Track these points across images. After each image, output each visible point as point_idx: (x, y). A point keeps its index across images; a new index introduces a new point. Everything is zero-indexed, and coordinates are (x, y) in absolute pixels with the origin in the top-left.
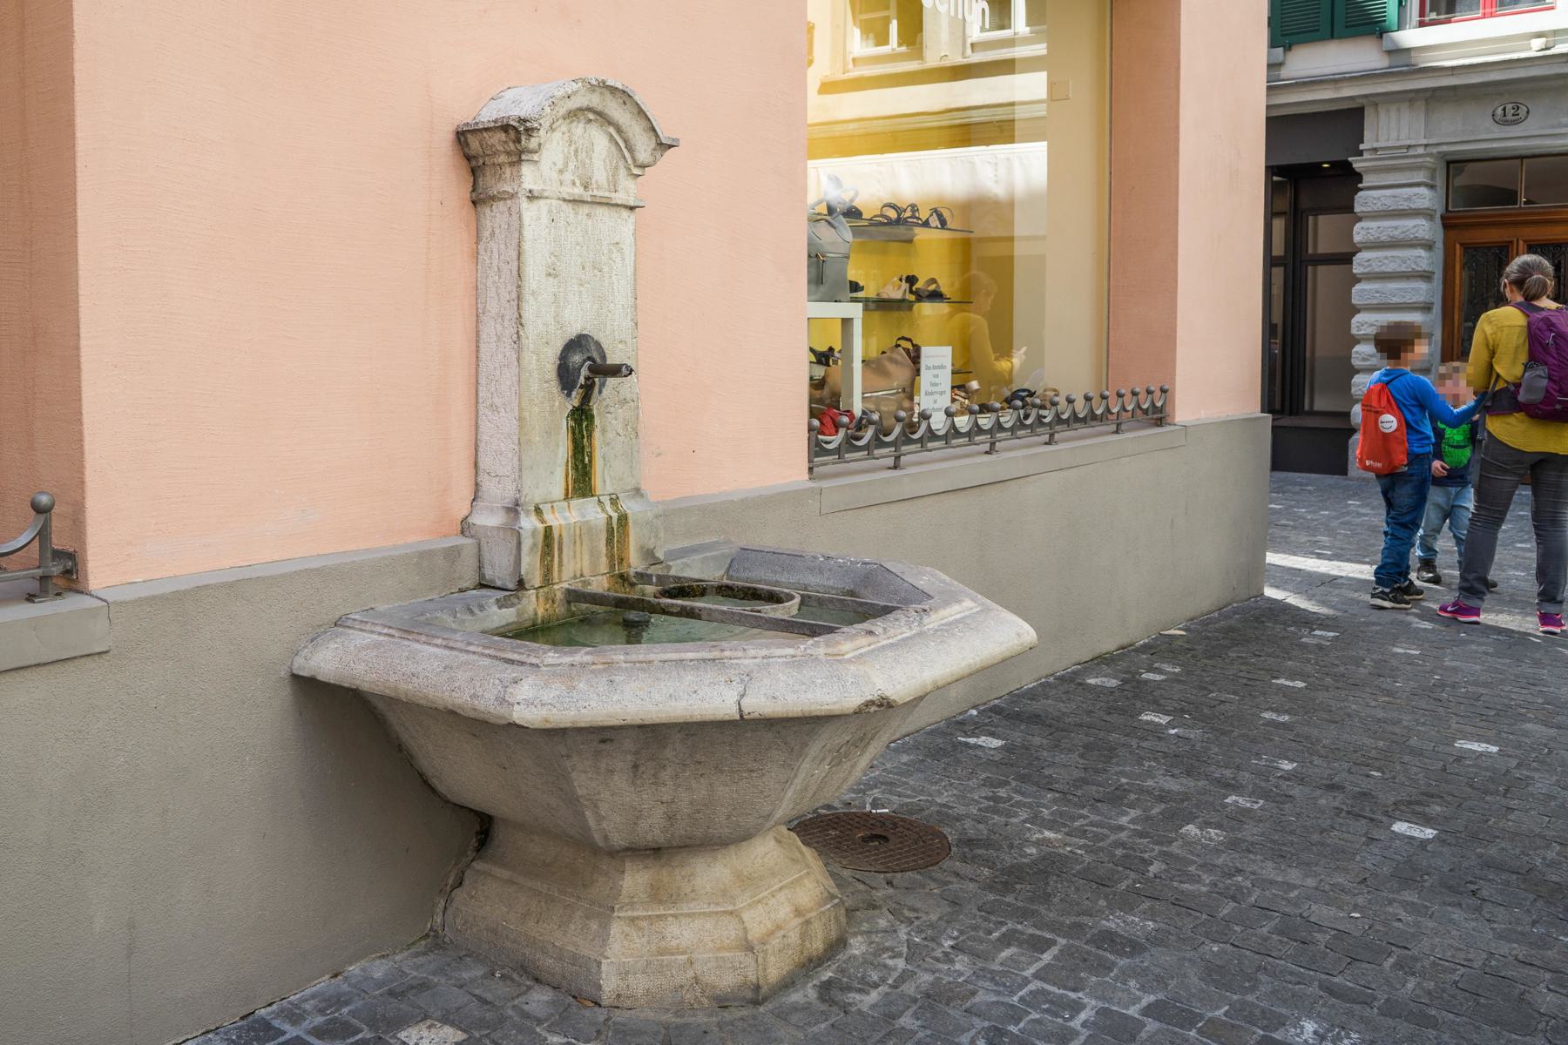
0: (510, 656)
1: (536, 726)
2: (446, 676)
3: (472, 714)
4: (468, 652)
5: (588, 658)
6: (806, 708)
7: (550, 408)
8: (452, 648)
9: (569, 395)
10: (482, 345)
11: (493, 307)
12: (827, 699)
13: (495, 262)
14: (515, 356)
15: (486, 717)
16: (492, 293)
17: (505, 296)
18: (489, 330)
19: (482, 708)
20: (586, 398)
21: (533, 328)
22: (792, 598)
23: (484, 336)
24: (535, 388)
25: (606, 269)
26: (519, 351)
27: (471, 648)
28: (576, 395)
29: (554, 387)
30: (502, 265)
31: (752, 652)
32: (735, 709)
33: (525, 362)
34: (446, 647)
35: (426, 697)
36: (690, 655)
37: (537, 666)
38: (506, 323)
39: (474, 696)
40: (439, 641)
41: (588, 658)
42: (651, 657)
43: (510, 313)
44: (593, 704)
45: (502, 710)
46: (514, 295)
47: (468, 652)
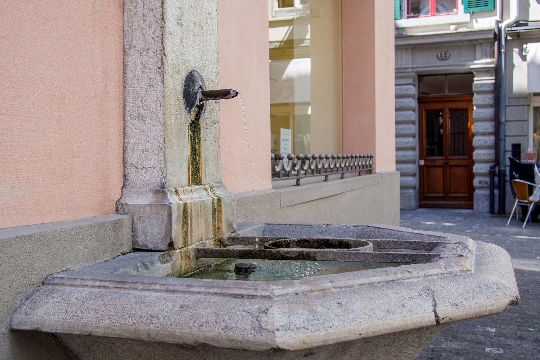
0: (236, 291)
1: (296, 348)
2: (187, 314)
3: (228, 345)
4: (192, 292)
5: (305, 288)
6: (477, 311)
7: (179, 117)
8: (173, 291)
9: (190, 111)
10: (129, 72)
11: (138, 43)
12: (488, 302)
13: (140, 10)
14: (159, 79)
15: (245, 346)
16: (138, 33)
17: (149, 33)
18: (135, 61)
19: (240, 338)
20: (198, 116)
21: (171, 59)
22: (367, 244)
23: (130, 65)
24: (172, 103)
25: (205, 29)
26: (163, 74)
27: (192, 289)
28: (194, 110)
29: (181, 104)
30: (147, 12)
31: (414, 273)
32: (433, 318)
33: (166, 82)
34: (167, 291)
35: (172, 334)
36: (376, 279)
37: (269, 297)
38: (151, 55)
39: (227, 328)
40: (158, 287)
41: (305, 288)
42: (350, 282)
43: (154, 47)
44: (336, 324)
45: (263, 338)
46: (158, 33)
47: (192, 292)
